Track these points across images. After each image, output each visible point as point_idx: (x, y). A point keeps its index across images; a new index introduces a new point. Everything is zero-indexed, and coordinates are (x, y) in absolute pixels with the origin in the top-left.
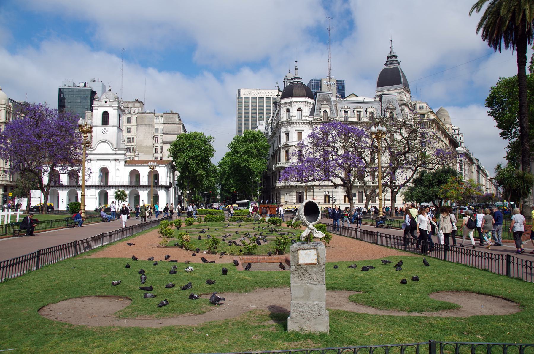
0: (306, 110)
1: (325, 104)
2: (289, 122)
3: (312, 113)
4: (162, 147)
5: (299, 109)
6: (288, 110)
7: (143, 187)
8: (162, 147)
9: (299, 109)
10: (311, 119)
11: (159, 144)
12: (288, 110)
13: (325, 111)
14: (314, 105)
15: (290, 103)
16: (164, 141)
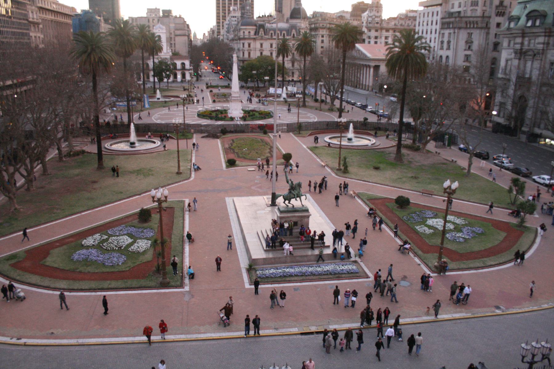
0: (252, 33)
1: (262, 30)
2: (244, 39)
3: (255, 34)
4: (174, 38)
5: (249, 32)
6: (244, 32)
7: (179, 70)
8: (174, 38)
9: (249, 32)
10: (255, 37)
11: (173, 36)
12: (244, 32)
13: (262, 34)
14: (256, 29)
15: (245, 29)
16: (176, 34)
